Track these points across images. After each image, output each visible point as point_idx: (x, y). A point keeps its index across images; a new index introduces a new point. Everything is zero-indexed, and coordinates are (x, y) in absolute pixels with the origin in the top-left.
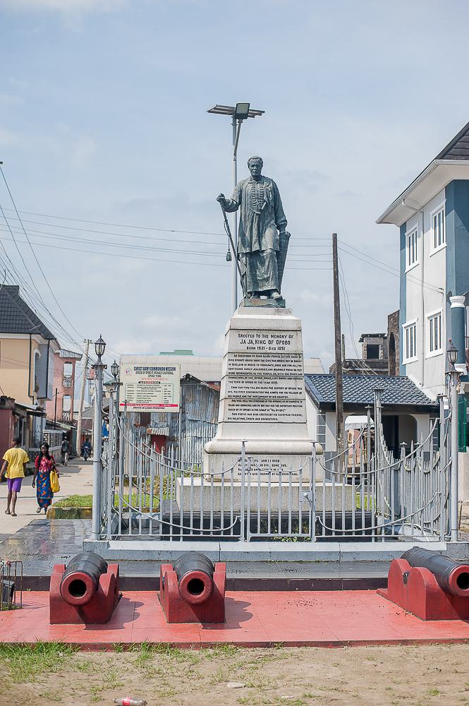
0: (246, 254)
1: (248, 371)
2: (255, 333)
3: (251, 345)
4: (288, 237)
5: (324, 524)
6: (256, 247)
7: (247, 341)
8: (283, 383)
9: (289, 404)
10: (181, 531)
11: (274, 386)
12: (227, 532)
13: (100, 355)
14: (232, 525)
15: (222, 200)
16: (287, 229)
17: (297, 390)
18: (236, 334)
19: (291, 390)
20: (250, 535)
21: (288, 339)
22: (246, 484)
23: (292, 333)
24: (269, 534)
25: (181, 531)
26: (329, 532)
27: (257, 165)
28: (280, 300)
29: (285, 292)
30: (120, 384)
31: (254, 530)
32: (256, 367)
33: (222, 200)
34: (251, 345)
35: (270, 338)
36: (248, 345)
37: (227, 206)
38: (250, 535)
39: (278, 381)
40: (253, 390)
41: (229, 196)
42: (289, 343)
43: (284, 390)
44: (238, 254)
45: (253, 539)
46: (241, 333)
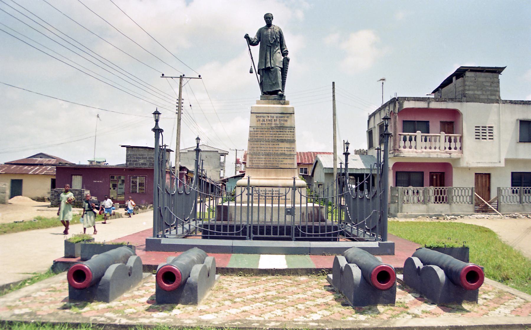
0: (263, 69)
1: (261, 138)
3: (264, 123)
4: (288, 60)
7: (261, 120)
8: (282, 145)
9: (286, 157)
10: (209, 233)
11: (277, 146)
12: (238, 234)
14: (241, 229)
15: (247, 37)
16: (288, 56)
17: (291, 149)
18: (255, 115)
19: (288, 149)
21: (286, 119)
23: (288, 115)
25: (209, 233)
26: (303, 235)
27: (268, 19)
28: (282, 96)
29: (287, 93)
31: (255, 233)
32: (266, 135)
33: (247, 37)
34: (264, 123)
35: (275, 118)
36: (261, 122)
38: (253, 235)
39: (280, 143)
40: (263, 149)
41: (253, 36)
42: (286, 121)
43: (283, 149)
44: (259, 70)
45: (255, 239)
46: (258, 115)
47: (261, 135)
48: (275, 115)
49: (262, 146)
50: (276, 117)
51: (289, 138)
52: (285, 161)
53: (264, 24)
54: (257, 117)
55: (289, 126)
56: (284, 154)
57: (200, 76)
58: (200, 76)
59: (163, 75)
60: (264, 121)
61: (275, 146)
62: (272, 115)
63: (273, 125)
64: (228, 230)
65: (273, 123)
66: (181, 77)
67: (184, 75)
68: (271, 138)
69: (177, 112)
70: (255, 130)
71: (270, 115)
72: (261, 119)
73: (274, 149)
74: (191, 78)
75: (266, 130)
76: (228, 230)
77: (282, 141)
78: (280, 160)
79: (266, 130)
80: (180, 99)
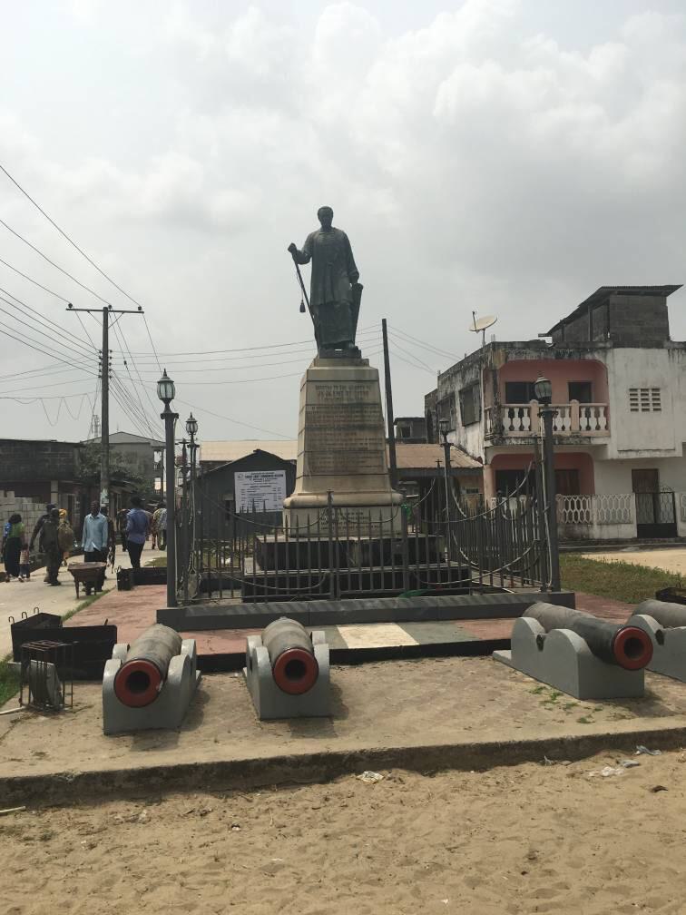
2: (330, 384)
4: (360, 287)
5: (419, 579)
6: (329, 298)
7: (325, 391)
8: (360, 434)
10: (266, 591)
11: (353, 437)
13: (167, 401)
15: (292, 248)
19: (372, 441)
20: (340, 592)
21: (366, 390)
22: (334, 539)
23: (368, 384)
24: (361, 590)
25: (266, 591)
27: (326, 215)
30: (188, 422)
33: (292, 248)
37: (299, 258)
38: (340, 592)
39: (358, 432)
40: (331, 442)
43: (364, 442)
46: (318, 384)
47: (326, 419)
48: (347, 385)
49: (328, 437)
50: (350, 388)
51: (372, 423)
52: (369, 462)
53: (317, 226)
54: (317, 388)
55: (370, 402)
56: (365, 450)
57: (140, 308)
58: (140, 308)
59: (70, 305)
60: (330, 394)
61: (350, 437)
62: (343, 384)
63: (345, 402)
64: (288, 585)
65: (345, 397)
66: (106, 311)
67: (110, 306)
68: (342, 423)
69: (101, 374)
70: (316, 410)
71: (338, 384)
72: (325, 391)
73: (349, 442)
74: (123, 312)
75: (334, 410)
76: (288, 585)
77: (362, 428)
78: (361, 460)
79: (334, 410)
80: (106, 350)
